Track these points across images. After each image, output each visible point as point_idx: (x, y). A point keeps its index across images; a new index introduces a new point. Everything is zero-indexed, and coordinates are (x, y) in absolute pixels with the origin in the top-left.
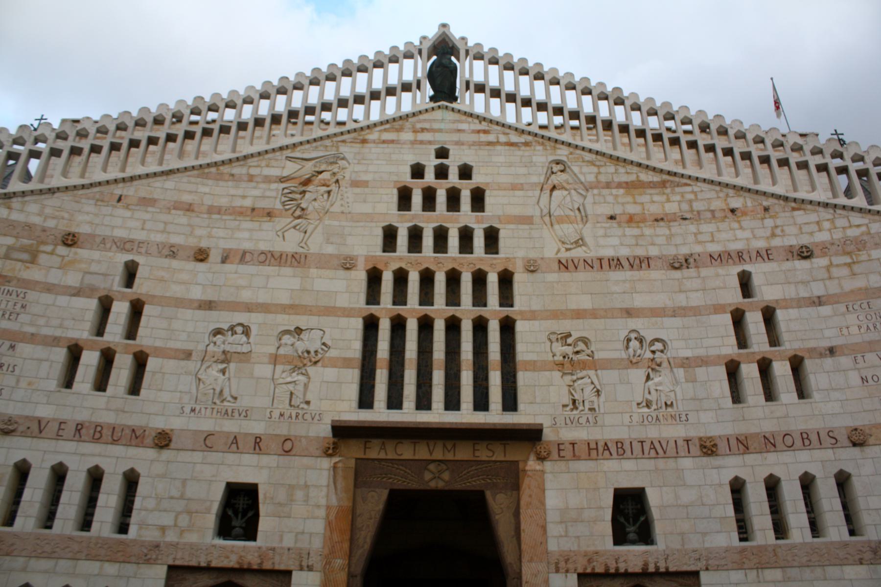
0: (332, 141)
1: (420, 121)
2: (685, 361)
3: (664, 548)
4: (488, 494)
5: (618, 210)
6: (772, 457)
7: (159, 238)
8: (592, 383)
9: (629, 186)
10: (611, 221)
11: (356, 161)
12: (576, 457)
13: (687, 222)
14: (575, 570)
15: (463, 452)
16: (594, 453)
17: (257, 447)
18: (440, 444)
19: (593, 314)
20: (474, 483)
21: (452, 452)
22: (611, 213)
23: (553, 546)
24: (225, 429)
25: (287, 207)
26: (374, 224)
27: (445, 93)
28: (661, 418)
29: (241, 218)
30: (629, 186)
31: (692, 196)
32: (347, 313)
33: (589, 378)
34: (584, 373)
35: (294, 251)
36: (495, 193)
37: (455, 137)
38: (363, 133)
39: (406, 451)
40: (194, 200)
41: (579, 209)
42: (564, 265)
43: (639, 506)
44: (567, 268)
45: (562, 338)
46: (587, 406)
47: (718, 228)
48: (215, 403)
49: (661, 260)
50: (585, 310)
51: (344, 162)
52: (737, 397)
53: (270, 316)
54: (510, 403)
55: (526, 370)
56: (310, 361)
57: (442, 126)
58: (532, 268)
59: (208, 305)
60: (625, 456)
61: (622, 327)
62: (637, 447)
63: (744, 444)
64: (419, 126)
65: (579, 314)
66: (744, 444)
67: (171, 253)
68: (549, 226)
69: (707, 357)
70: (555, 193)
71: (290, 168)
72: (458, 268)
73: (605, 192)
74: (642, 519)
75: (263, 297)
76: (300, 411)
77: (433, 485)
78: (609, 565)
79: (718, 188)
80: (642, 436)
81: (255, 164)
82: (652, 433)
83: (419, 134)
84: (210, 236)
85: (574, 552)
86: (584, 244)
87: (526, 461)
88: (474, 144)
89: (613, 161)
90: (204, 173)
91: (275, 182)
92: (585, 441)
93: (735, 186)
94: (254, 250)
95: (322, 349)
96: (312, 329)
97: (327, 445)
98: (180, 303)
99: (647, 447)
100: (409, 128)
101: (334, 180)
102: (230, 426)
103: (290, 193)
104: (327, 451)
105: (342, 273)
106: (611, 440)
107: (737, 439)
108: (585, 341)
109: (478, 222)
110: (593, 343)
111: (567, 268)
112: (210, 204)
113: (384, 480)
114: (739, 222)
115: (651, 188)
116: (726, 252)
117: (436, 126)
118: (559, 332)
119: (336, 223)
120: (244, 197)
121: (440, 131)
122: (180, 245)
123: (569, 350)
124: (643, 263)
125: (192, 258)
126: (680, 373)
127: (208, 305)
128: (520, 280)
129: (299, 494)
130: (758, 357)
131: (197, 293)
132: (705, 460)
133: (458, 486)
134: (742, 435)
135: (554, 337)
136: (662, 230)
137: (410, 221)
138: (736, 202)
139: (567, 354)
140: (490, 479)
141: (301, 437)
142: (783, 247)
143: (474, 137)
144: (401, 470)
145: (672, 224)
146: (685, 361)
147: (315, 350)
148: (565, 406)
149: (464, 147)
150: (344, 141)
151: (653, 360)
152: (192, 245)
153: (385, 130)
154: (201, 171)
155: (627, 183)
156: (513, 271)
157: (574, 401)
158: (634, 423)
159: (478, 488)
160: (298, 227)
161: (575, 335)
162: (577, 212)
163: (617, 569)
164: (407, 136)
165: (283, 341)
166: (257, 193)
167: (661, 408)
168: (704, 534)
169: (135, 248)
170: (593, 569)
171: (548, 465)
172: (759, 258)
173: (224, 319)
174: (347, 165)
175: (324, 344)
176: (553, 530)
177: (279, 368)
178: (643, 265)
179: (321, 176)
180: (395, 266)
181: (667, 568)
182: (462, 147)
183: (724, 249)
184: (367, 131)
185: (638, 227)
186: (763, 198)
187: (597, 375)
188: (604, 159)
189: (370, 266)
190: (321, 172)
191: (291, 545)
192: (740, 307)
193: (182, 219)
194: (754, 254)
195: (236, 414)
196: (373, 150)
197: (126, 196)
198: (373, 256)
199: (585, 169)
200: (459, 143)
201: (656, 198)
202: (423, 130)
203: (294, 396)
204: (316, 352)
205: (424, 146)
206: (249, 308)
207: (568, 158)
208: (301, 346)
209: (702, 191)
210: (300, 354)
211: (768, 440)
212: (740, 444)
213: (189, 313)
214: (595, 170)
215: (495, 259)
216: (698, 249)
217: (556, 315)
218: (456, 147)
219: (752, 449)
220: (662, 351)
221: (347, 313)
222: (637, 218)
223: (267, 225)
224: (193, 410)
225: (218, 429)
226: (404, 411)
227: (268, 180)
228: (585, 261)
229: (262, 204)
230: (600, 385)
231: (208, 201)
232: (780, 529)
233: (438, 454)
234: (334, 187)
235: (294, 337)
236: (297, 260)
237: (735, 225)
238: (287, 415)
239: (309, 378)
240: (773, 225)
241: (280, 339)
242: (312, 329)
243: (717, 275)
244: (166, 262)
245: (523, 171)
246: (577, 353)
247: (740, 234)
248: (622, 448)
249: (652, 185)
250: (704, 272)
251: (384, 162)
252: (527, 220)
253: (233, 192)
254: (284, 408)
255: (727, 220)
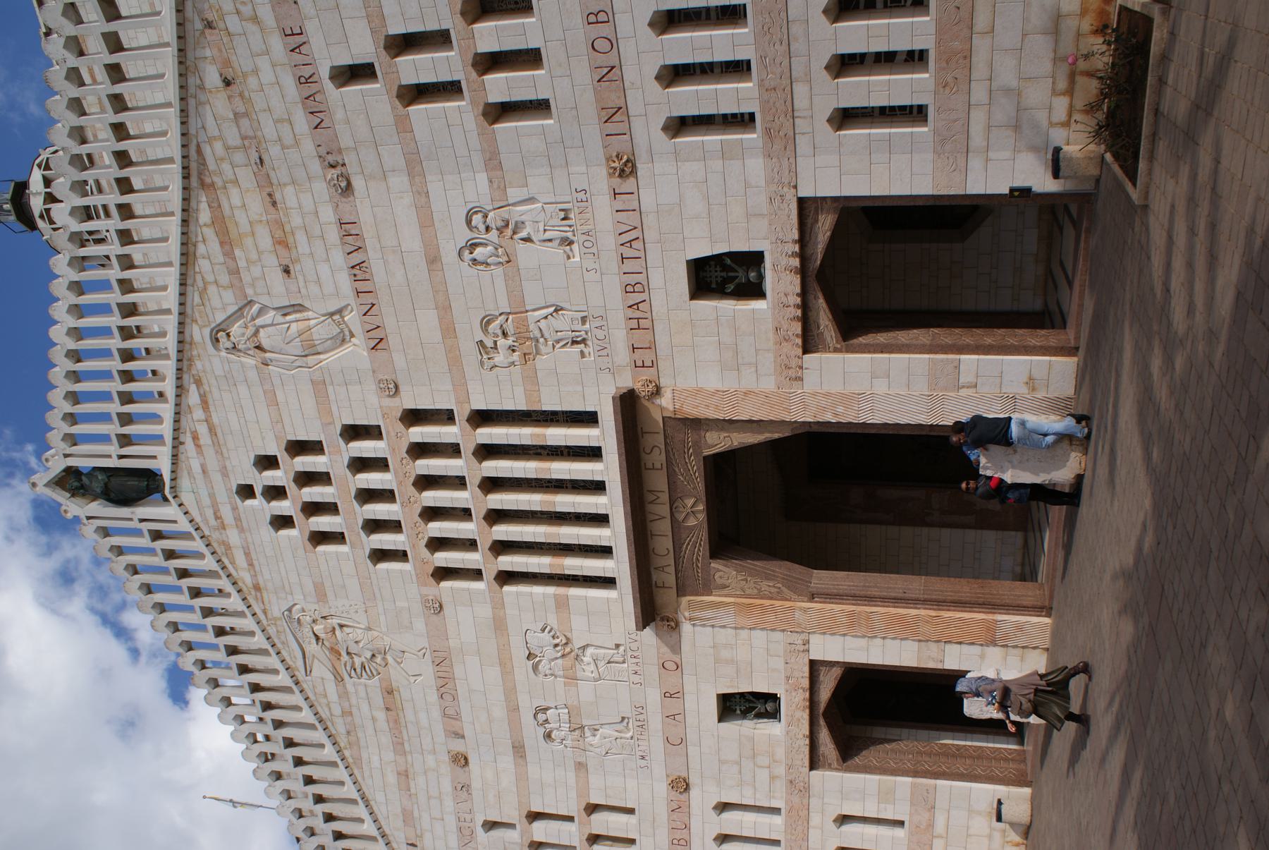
0: (269, 625)
1: (206, 521)
2: (495, 186)
3: (767, 242)
4: (707, 452)
5: (271, 261)
6: (630, 74)
7: (449, 804)
8: (546, 318)
9: (227, 243)
10: (292, 272)
11: (289, 597)
12: (652, 346)
13: (263, 157)
14: (799, 357)
15: (658, 481)
16: (643, 323)
17: (675, 696)
18: (650, 508)
19: (444, 309)
20: (695, 468)
21: (659, 494)
22: (279, 272)
23: (768, 384)
24: (660, 727)
25: (375, 673)
26: (373, 576)
27: (148, 485)
28: (585, 228)
29: (402, 720)
30: (227, 243)
31: (218, 146)
32: (499, 605)
33: (539, 321)
34: (532, 327)
35: (431, 663)
36: (288, 428)
37: (216, 477)
38: (245, 589)
39: (663, 543)
40: (392, 771)
41: (285, 315)
42: (378, 344)
43: (714, 286)
44: (382, 339)
45: (487, 353)
46: (579, 327)
47: (265, 110)
48: (632, 738)
49: (339, 204)
50: (440, 319)
51: (294, 609)
52: (540, 107)
53: (519, 688)
54: (589, 419)
55: (540, 401)
56: (566, 644)
57: (204, 493)
58: (391, 386)
59: (519, 750)
60: (645, 283)
61: (457, 272)
62: (630, 266)
63: (614, 114)
64: (213, 522)
65: (449, 330)
66: (614, 114)
67: (464, 789)
68: (322, 357)
69: (483, 151)
70: (265, 343)
71: (321, 671)
72: (412, 479)
73: (246, 278)
74: (728, 261)
75: (497, 695)
76: (630, 653)
77: (702, 517)
78: (792, 316)
79: (192, 102)
80: (615, 259)
81: (326, 710)
82: (608, 242)
83: (225, 523)
84: (434, 752)
85: (775, 357)
86: (340, 311)
87: (662, 409)
88: (219, 452)
89: (191, 261)
90: (355, 763)
91: (344, 686)
92: (628, 333)
93: (180, 75)
94: (440, 706)
95: (549, 632)
96: (527, 643)
97: (665, 627)
98: (521, 778)
99: (628, 252)
100: (221, 534)
101: (323, 620)
102: (655, 722)
103: (355, 670)
104: (672, 628)
105: (447, 610)
106: (624, 300)
107: (606, 122)
108: (486, 323)
109: (340, 452)
110: (487, 313)
111: (382, 339)
112: (392, 754)
113: (700, 565)
114: (245, 75)
115: (220, 206)
116: (303, 104)
117: (206, 501)
118: (480, 357)
119: (382, 618)
120: (374, 719)
121: (212, 496)
122: (453, 781)
123: (501, 342)
124: (348, 229)
125: (467, 769)
126: (514, 194)
127: (519, 750)
128: (411, 400)
129: (725, 654)
130: (474, 74)
131: (507, 762)
132: (642, 169)
133: (701, 486)
134: (599, 115)
135: (488, 364)
136: (288, 196)
137: (359, 533)
138: (212, 77)
139: (510, 347)
140: (689, 450)
141: (658, 653)
142: (273, 6)
143: (209, 452)
144: (687, 548)
145: (275, 181)
146: (495, 186)
147: (551, 639)
148: (582, 354)
149: (227, 463)
150: (265, 612)
151: (500, 230)
152: (449, 769)
153: (233, 563)
154: (352, 766)
155: (222, 244)
156: (401, 411)
157: (574, 342)
158: (597, 266)
159: (702, 463)
160: (399, 660)
161: (480, 336)
162: (289, 318)
163: (797, 306)
164: (233, 537)
165: (548, 672)
166: (365, 707)
167: (570, 226)
168: (747, 185)
169: (467, 824)
170: (797, 335)
171: (663, 382)
172: (304, 49)
173: (531, 733)
174: (297, 607)
175: (543, 630)
176: (748, 381)
177: (580, 674)
178: (353, 232)
179: (322, 636)
180: (425, 553)
181: (795, 242)
182: (229, 468)
183: (300, 105)
184: (240, 584)
185: (293, 234)
186: (188, 26)
187: (534, 310)
188: (190, 273)
189: (432, 580)
190: (317, 638)
191: (782, 661)
192: (394, 93)
193: (419, 783)
194: (297, 58)
195: (641, 717)
196: (267, 576)
197: (406, 838)
198: (418, 578)
199: (216, 302)
200: (225, 473)
201: (236, 201)
202: (217, 518)
203: (612, 660)
204: (553, 637)
205: (242, 516)
206: (513, 709)
207: (204, 326)
208: (550, 652)
209: (203, 127)
210: (559, 654)
211: (603, 77)
212: (613, 119)
213: (533, 770)
214: (212, 290)
215: (388, 433)
216: (308, 146)
217: (455, 361)
218: (231, 476)
219: (621, 103)
220: (486, 216)
221: (499, 605)
222: (279, 234)
223: (405, 694)
224: (643, 758)
225: (661, 734)
226: (613, 544)
227: (343, 695)
228: (365, 315)
229: (378, 699)
230: (547, 307)
231: (389, 756)
232: (738, 68)
233: (664, 510)
234: (335, 622)
235: (540, 661)
236: (442, 662)
237: (252, 82)
238: (636, 668)
239: (588, 645)
240: (236, 18)
241: (546, 675)
242: (527, 643)
243: (348, 121)
244: (476, 794)
245: (243, 389)
246: (505, 334)
247: (267, 75)
248: (633, 286)
249: (215, 207)
250: (345, 141)
251: (281, 565)
252: (320, 387)
253: (370, 731)
254: (628, 671)
255: (246, 94)
